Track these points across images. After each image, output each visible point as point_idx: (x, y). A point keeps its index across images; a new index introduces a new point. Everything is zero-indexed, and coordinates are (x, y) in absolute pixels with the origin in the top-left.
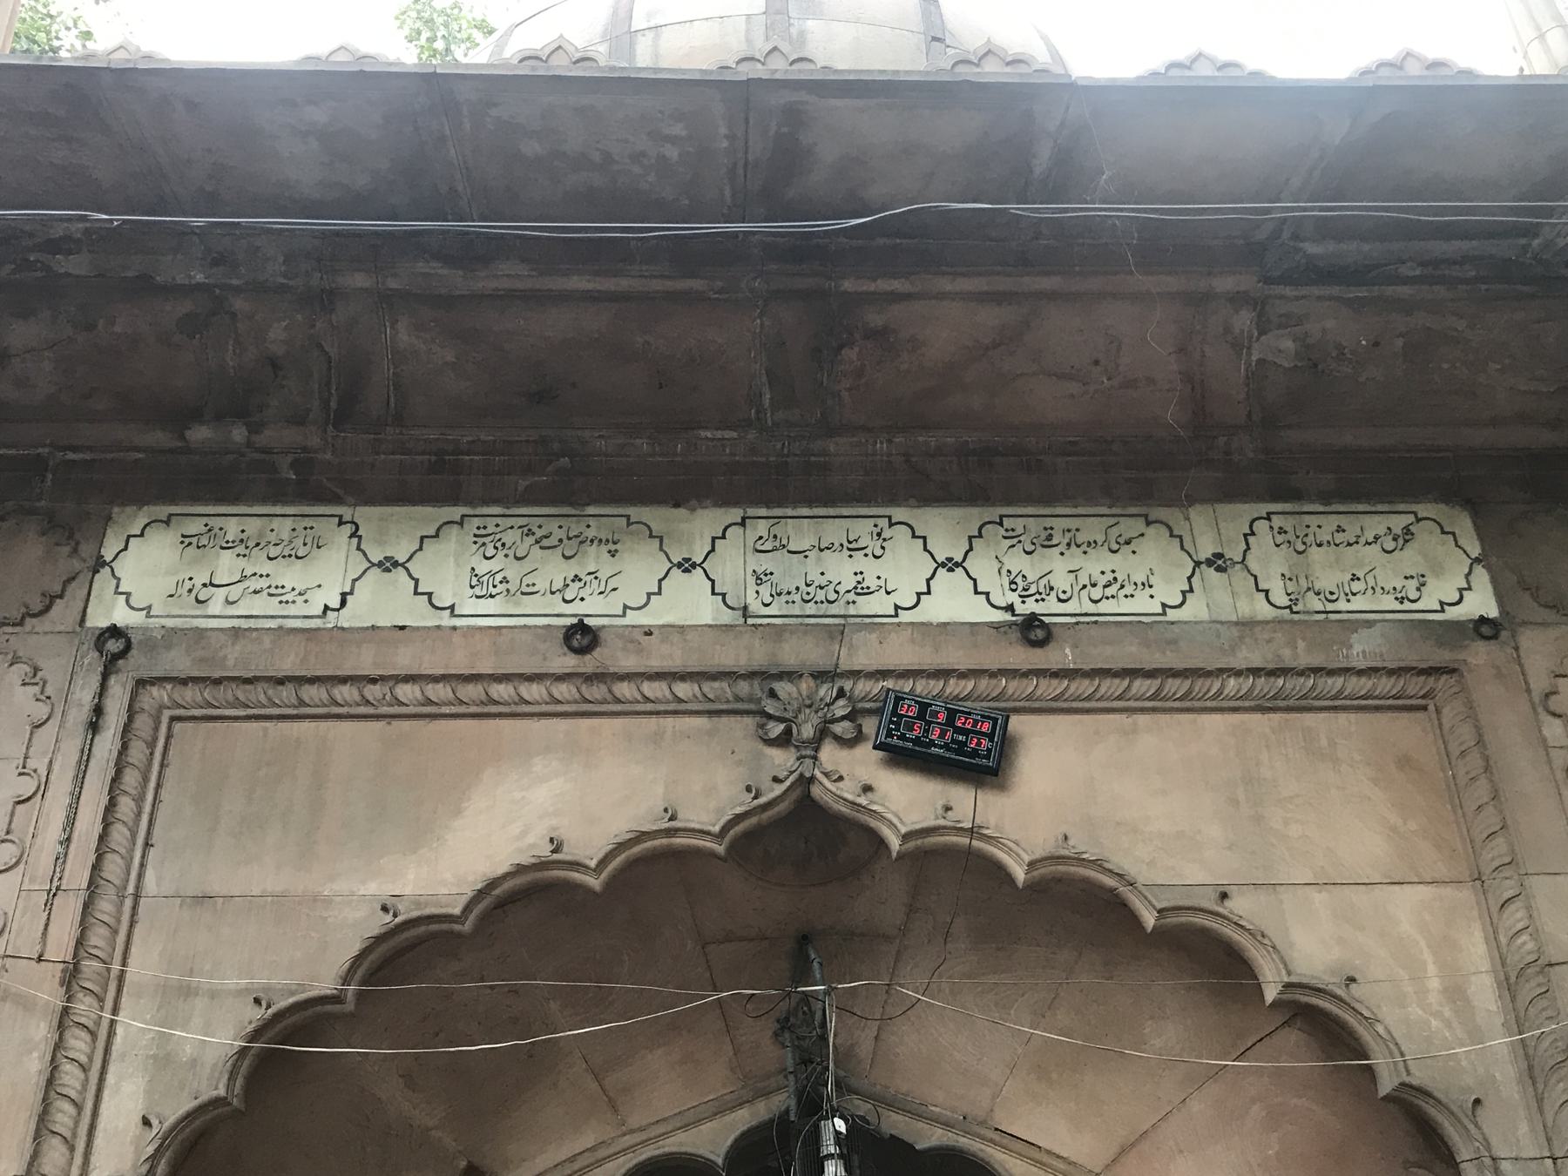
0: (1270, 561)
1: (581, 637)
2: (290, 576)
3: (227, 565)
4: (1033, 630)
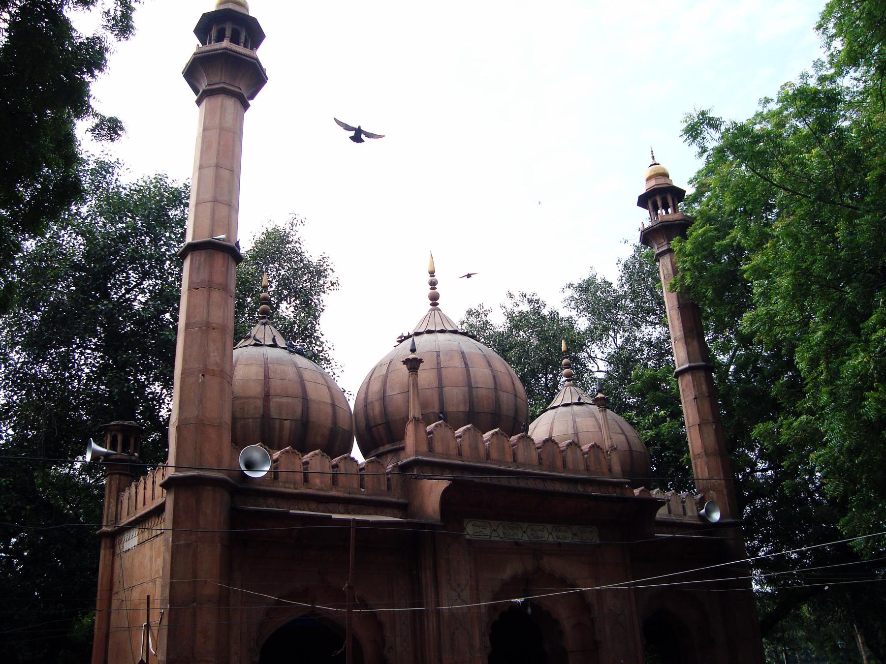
1: (517, 543)
4: (559, 544)
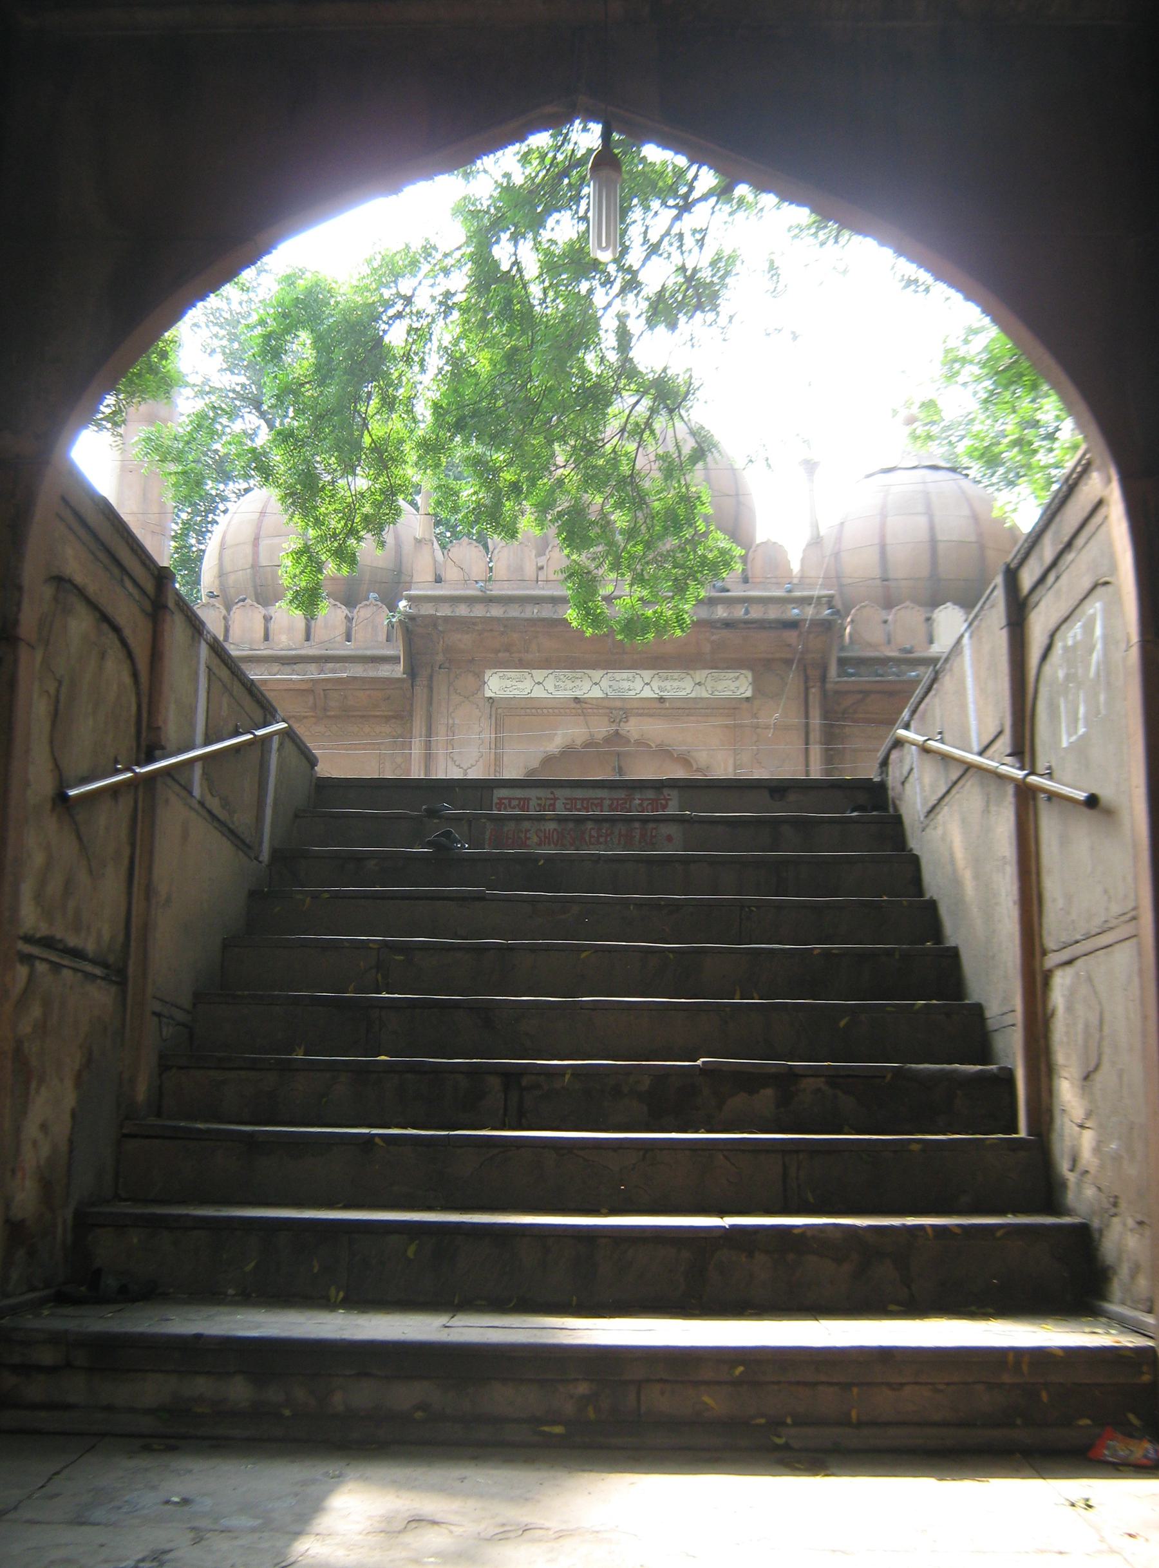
0: (710, 684)
1: (577, 700)
2: (520, 685)
3: (509, 683)
4: (661, 700)
